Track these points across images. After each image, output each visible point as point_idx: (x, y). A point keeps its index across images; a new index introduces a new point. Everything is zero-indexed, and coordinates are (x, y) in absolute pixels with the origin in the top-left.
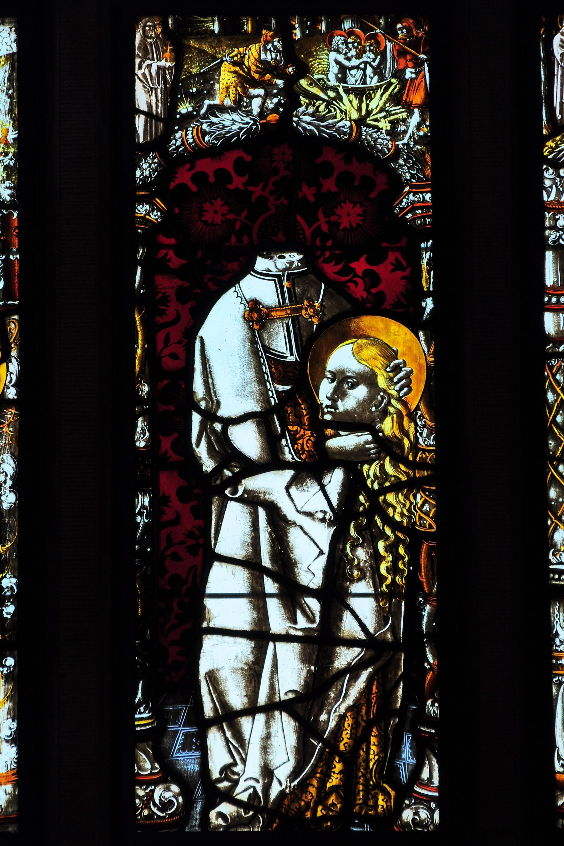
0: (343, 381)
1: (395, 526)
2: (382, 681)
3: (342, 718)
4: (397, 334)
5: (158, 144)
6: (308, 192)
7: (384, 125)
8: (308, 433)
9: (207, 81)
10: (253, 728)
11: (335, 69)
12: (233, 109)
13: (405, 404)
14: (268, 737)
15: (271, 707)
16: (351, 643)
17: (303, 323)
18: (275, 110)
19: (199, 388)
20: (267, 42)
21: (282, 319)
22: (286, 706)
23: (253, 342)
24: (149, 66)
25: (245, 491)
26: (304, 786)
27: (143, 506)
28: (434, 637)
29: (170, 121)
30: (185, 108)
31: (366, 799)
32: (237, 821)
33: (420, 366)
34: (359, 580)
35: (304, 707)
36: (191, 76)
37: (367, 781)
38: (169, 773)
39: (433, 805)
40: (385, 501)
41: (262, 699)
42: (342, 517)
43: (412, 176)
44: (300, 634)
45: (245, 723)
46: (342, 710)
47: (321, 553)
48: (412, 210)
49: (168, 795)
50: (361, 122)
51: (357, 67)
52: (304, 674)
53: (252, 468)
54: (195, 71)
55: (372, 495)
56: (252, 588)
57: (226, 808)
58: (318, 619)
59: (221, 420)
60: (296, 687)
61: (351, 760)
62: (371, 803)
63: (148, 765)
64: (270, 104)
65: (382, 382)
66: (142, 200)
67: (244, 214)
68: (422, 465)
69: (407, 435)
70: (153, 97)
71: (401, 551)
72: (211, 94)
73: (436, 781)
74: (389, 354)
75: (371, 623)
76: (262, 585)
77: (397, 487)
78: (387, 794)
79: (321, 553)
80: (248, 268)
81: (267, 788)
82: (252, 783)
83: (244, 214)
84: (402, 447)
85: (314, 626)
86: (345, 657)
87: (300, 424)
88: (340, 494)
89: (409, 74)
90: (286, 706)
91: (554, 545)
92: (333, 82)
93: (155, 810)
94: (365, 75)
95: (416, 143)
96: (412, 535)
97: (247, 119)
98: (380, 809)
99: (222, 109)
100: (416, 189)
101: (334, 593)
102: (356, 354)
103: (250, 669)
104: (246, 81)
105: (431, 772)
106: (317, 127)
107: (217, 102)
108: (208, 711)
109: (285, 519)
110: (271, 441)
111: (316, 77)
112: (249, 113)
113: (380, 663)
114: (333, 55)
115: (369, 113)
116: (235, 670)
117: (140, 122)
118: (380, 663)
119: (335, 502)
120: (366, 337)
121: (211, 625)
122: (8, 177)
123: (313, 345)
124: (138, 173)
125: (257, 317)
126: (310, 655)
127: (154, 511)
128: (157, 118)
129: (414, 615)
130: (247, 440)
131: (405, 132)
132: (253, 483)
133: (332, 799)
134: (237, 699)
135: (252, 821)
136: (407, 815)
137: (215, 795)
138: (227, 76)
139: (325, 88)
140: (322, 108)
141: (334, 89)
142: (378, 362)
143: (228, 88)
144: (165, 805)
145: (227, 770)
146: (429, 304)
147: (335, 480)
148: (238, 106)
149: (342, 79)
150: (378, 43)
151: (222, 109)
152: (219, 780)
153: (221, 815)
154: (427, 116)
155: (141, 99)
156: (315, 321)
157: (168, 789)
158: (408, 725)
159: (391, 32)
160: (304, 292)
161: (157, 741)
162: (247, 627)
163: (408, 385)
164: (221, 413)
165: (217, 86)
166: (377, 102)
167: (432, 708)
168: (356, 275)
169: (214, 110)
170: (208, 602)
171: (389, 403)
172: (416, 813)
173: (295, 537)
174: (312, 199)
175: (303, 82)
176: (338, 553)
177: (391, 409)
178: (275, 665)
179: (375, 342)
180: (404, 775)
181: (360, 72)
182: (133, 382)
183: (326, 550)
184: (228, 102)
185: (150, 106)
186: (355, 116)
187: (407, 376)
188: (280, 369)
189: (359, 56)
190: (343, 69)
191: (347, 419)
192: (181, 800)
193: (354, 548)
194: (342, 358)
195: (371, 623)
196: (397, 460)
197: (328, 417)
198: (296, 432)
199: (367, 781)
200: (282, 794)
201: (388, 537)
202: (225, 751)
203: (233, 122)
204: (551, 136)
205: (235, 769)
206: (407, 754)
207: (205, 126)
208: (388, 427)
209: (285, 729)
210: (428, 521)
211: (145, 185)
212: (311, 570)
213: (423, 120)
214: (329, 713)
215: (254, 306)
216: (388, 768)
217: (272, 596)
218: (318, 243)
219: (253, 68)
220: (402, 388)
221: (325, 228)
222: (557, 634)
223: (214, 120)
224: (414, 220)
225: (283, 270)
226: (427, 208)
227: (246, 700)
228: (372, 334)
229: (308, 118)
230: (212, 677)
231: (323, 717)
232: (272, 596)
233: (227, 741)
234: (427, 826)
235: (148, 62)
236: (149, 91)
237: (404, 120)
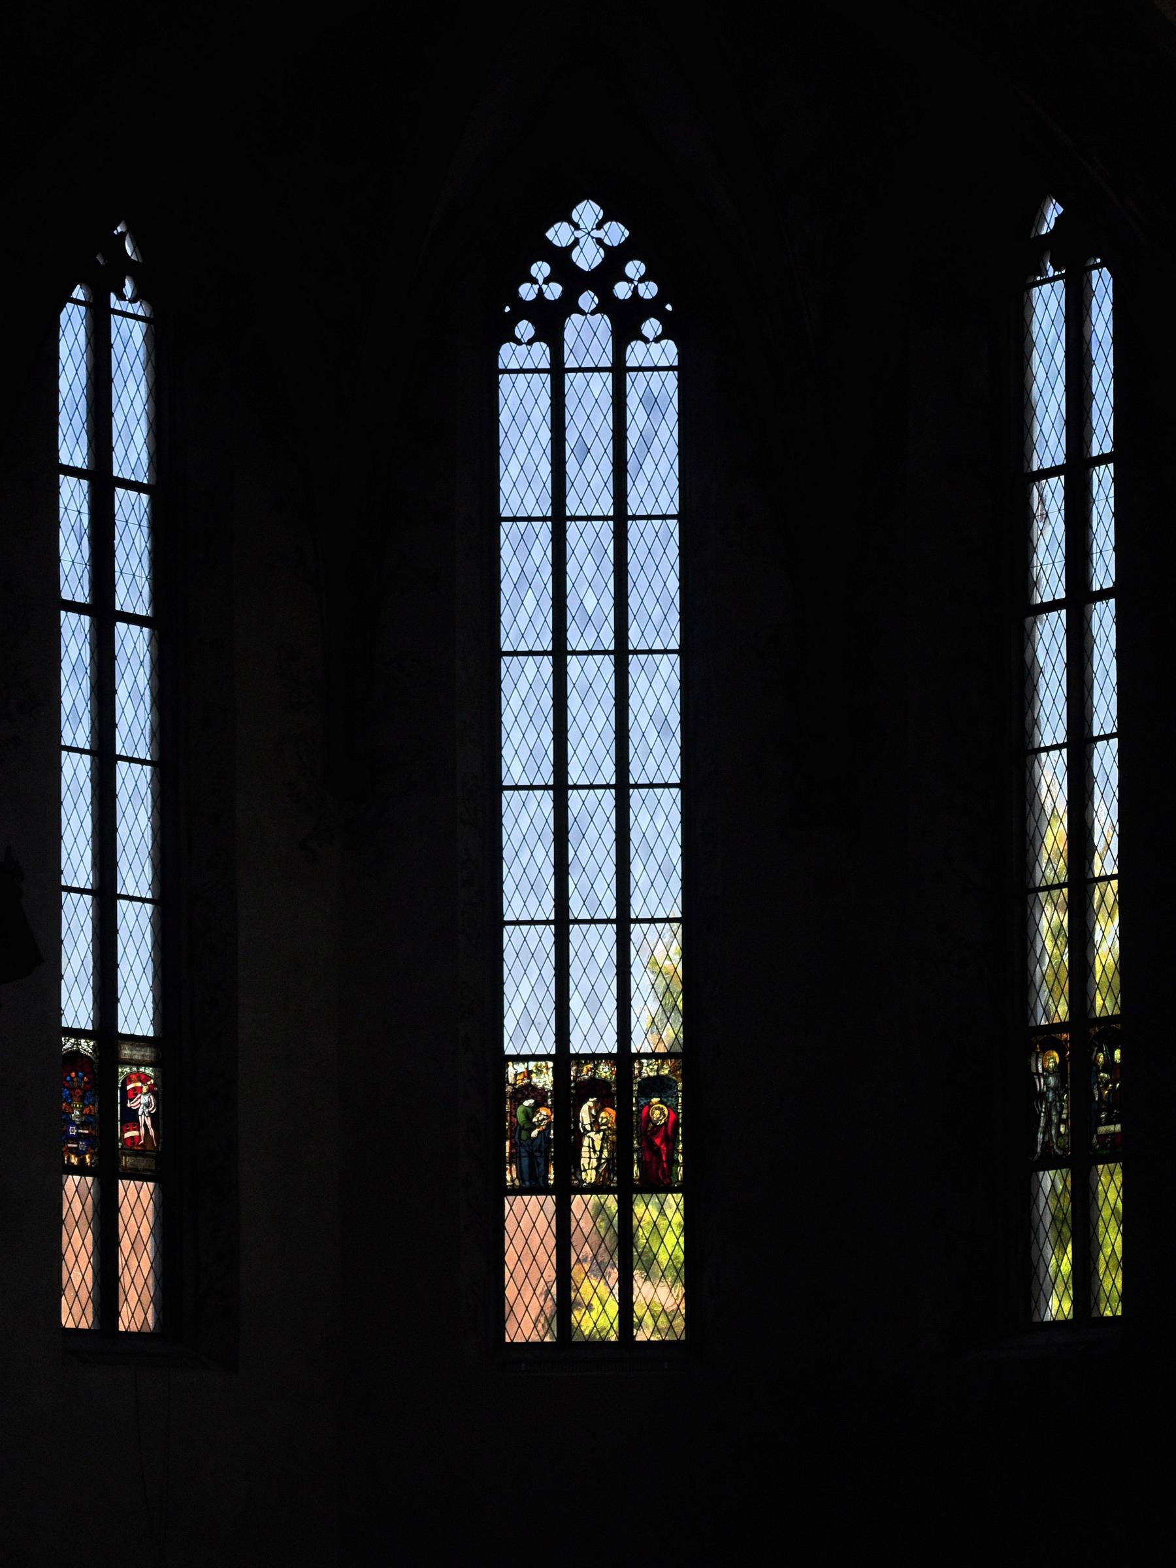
5: (574, 1080)
35: (597, 1169)
42: (602, 1139)
101: (601, 1151)
123: (598, 1112)
130: (588, 1128)
142: (608, 1115)
194: (603, 1114)
212: (598, 1148)
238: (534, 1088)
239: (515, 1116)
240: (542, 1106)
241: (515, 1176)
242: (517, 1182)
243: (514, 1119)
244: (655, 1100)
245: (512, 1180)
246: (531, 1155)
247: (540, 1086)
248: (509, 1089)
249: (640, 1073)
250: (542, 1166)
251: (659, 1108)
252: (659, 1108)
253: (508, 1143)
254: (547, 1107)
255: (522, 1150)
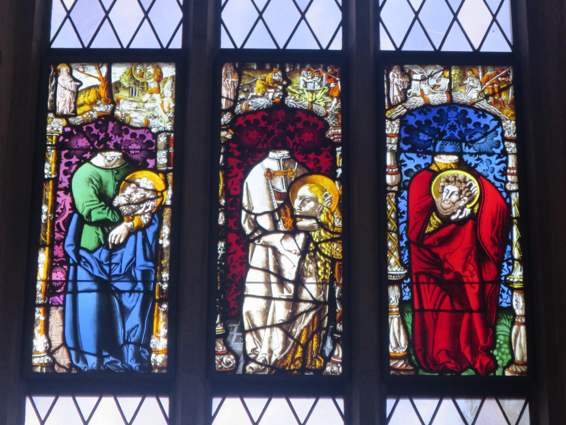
0: (304, 200)
1: (325, 256)
2: (319, 316)
3: (302, 331)
4: (326, 182)
5: (231, 109)
6: (291, 128)
7: (322, 104)
8: (290, 220)
9: (251, 86)
10: (265, 334)
11: (302, 83)
12: (261, 97)
13: (329, 209)
14: (271, 337)
15: (272, 326)
16: (306, 301)
17: (288, 178)
18: (278, 97)
19: (245, 201)
20: (275, 73)
21: (279, 175)
22: (279, 326)
23: (268, 184)
24: (228, 81)
25: (263, 242)
26: (285, 357)
27: (221, 247)
28: (340, 299)
29: (236, 101)
30: (242, 96)
31: (311, 363)
32: (258, 370)
33: (336, 195)
34: (310, 277)
35: (286, 326)
36: (244, 85)
37: (312, 356)
38: (230, 351)
39: (339, 365)
40: (321, 246)
41: (269, 323)
42: (304, 252)
43: (333, 123)
44: (285, 297)
45: (262, 332)
46: (302, 327)
47: (294, 266)
48: (333, 135)
49: (229, 360)
50: (312, 102)
51: (311, 82)
52: (286, 313)
53: (266, 233)
54: (246, 83)
55: (316, 244)
56: (266, 279)
57: (253, 365)
58: (293, 292)
59: (254, 214)
60: (283, 318)
61: (305, 347)
62: (313, 364)
63: (221, 348)
64: (277, 95)
65: (320, 201)
66: (224, 130)
67: (265, 135)
68: (337, 233)
69: (330, 221)
70: (229, 92)
71: (327, 266)
72: (252, 91)
73: (341, 356)
74: (323, 190)
75: (314, 294)
76: (270, 278)
77: (326, 241)
78: (320, 360)
79: (294, 266)
80: (266, 156)
81: (270, 358)
82: (264, 355)
83: (265, 135)
84: (328, 226)
85: (291, 294)
86: (303, 307)
87: (286, 216)
88: (303, 244)
89: (332, 85)
90: (279, 326)
91: (390, 264)
92: (301, 87)
93: (224, 365)
94: (314, 86)
95: (335, 111)
96: (333, 261)
97: (267, 101)
98: (317, 367)
99: (257, 97)
100: (335, 127)
101: (299, 282)
102: (310, 189)
103: (264, 311)
104: (267, 86)
105: (339, 352)
106: (295, 104)
107: (255, 94)
108: (246, 327)
109: (279, 253)
110: (275, 223)
111: (295, 85)
112: (268, 98)
113: (318, 309)
114: (302, 78)
115: (316, 99)
116: (258, 311)
117: (223, 101)
118: (318, 309)
119: (300, 246)
120: (314, 183)
121: (248, 294)
122: (170, 121)
123: (292, 186)
124: (222, 120)
125: (270, 174)
126: (289, 306)
127: (226, 248)
128: (231, 100)
129: (332, 291)
130: (265, 222)
131: (330, 107)
132: (266, 239)
133: (297, 362)
134: (258, 322)
135: (264, 370)
136: (328, 369)
137: (248, 360)
138: (259, 85)
139: (298, 90)
140: (297, 97)
141: (302, 90)
142: (319, 196)
143: (259, 89)
144: (228, 363)
145: (254, 350)
146: (339, 171)
147: (301, 238)
148: (263, 95)
149: (306, 87)
150: (320, 74)
151: (257, 97)
152: (250, 354)
153: (251, 368)
154: (339, 100)
155: (224, 92)
156: (293, 177)
157: (229, 357)
158: (329, 334)
159: (325, 70)
160: (289, 166)
161: (225, 337)
162: (263, 295)
163: (331, 202)
164: (254, 211)
165: (255, 88)
166: (319, 95)
167: (339, 327)
168: (310, 160)
169: (253, 97)
170: (247, 285)
171: (323, 209)
172: (332, 368)
173: (283, 260)
174: (293, 130)
175: (290, 87)
176: (301, 267)
177: (324, 211)
178: (274, 310)
179: (318, 185)
180: (327, 353)
181: (313, 84)
182: (218, 199)
183: (297, 265)
184: (259, 94)
185: (228, 96)
186: (310, 100)
187: (331, 199)
188: (279, 195)
189: (312, 78)
190: (306, 83)
191: (306, 215)
192: (234, 361)
193: (308, 264)
194: (304, 191)
195: (314, 294)
196: (326, 230)
197: (298, 214)
198: (285, 219)
199: (312, 356)
200: (277, 360)
201: (322, 261)
202: (253, 343)
203: (262, 102)
204: (389, 109)
205: (257, 350)
206: (329, 345)
207: (250, 103)
208: (322, 218)
209: (278, 335)
210: (338, 255)
211: (225, 125)
212: (290, 273)
213: (338, 102)
214: (296, 329)
215: (268, 170)
216: (321, 352)
217: (274, 283)
218: (295, 147)
219: (270, 82)
220: (328, 203)
221: (298, 141)
222: (391, 299)
223: (254, 101)
224: (334, 139)
225: (281, 157)
226: (339, 135)
227: (262, 323)
228: (317, 182)
229: (291, 101)
230: (248, 314)
231: (294, 330)
232: (274, 283)
233: (254, 339)
234: (336, 373)
235: (227, 79)
236: (228, 90)
237: (330, 102)
238: (123, 126)
239: (68, 190)
240: (144, 167)
241: (57, 341)
242: (62, 358)
243: (63, 198)
244: (443, 160)
245: (50, 352)
246: (105, 288)
247: (138, 119)
248: (55, 126)
249: (405, 95)
250: (134, 319)
251: (455, 180)
252: (455, 180)
253: (43, 257)
254: (155, 170)
255: (82, 274)
